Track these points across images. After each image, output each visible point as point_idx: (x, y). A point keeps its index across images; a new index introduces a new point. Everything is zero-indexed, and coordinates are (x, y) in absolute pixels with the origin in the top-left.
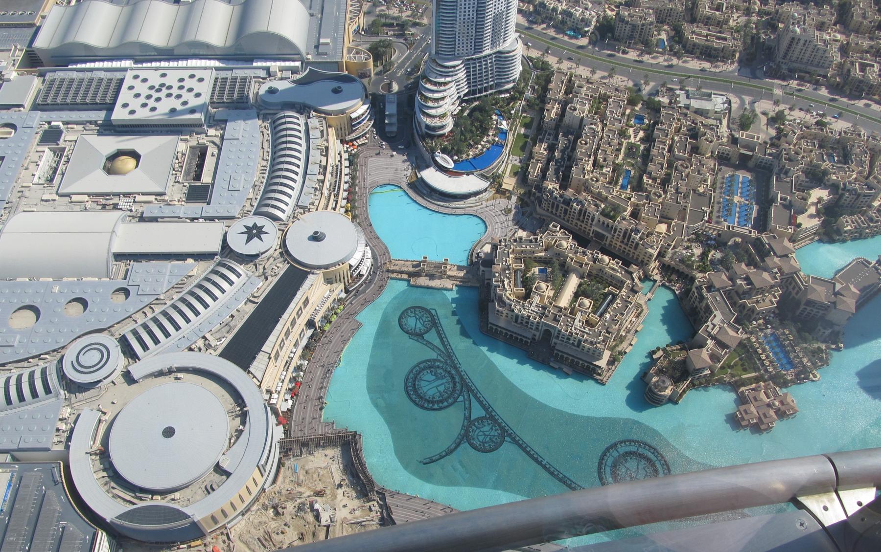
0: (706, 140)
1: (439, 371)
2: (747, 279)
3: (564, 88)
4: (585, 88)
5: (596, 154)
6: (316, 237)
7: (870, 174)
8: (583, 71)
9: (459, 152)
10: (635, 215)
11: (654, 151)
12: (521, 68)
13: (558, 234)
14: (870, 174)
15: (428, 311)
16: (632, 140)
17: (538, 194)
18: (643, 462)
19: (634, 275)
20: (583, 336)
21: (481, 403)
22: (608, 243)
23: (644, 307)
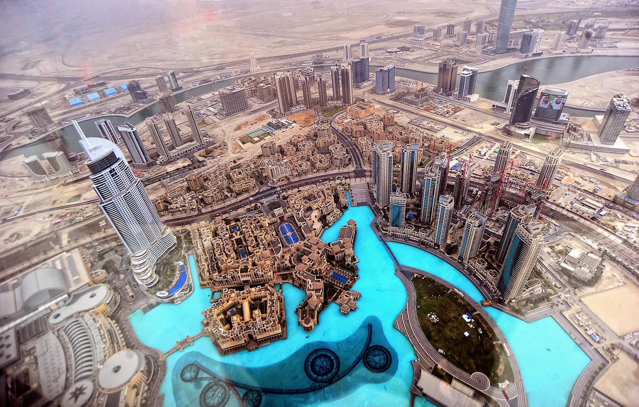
0: (263, 221)
1: (215, 387)
2: (310, 260)
3: (198, 234)
4: (206, 230)
5: (224, 252)
6: (117, 369)
7: (325, 197)
8: (203, 223)
9: (167, 287)
10: (254, 264)
11: (247, 237)
12: (175, 237)
13: (229, 292)
14: (325, 197)
15: (192, 364)
16: (236, 238)
17: (211, 282)
18: (322, 359)
19: (269, 288)
20: (264, 326)
21: (241, 387)
22: (251, 282)
23: (281, 296)
